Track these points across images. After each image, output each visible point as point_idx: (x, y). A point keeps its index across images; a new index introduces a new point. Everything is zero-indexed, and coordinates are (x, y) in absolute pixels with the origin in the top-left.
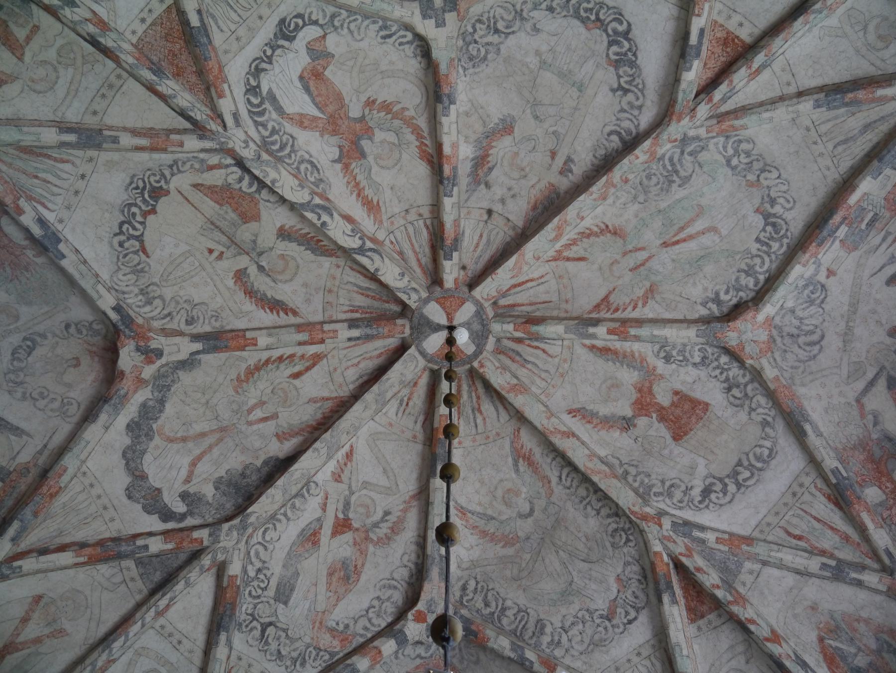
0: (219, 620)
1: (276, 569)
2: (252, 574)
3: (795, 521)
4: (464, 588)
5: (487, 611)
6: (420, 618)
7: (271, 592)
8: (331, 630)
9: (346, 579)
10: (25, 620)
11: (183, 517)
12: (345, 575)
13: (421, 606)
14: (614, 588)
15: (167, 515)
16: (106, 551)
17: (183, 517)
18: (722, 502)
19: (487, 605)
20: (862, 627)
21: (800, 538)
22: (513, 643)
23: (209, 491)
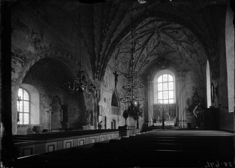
12: (154, 43)
23: (144, 43)
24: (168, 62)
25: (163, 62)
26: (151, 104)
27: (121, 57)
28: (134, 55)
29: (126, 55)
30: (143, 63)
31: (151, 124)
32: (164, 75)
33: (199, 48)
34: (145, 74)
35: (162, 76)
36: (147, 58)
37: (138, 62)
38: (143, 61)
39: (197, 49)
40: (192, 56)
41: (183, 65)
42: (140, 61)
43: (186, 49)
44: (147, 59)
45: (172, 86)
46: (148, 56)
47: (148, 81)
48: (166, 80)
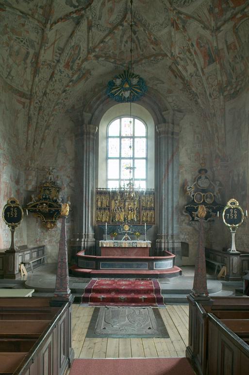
0: (90, 27)
1: (98, 13)
2: (93, 16)
3: (200, 12)
4: (135, 13)
5: (139, 19)
6: (126, 21)
7: (98, 18)
8: (110, 24)
9: (112, 11)
10: (56, 35)
11: (78, 6)
12: (111, 10)
13: (126, 19)
14: (164, 19)
15: (75, 7)
16: (66, 17)
17: (78, 6)
18: (187, 5)
19: (139, 17)
20: (205, 38)
21: (200, 17)
22: (144, 29)
24: (138, 82)
25: (124, 87)
26: (90, 189)
27: (6, 26)
28: (51, 35)
29: (23, 25)
30: (73, 75)
31: (88, 240)
32: (123, 119)
33: (229, 48)
34: (76, 107)
35: (119, 120)
36: (86, 59)
37: (61, 66)
38: (75, 67)
39: (225, 49)
40: (206, 70)
41: (174, 98)
42: (67, 65)
43: (195, 46)
44: (86, 65)
45: (142, 147)
46: (89, 53)
47: (84, 126)
48: (127, 131)
